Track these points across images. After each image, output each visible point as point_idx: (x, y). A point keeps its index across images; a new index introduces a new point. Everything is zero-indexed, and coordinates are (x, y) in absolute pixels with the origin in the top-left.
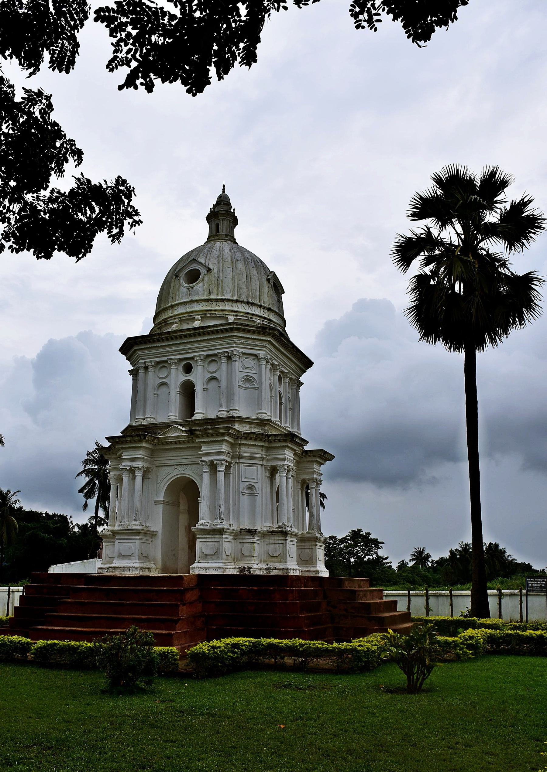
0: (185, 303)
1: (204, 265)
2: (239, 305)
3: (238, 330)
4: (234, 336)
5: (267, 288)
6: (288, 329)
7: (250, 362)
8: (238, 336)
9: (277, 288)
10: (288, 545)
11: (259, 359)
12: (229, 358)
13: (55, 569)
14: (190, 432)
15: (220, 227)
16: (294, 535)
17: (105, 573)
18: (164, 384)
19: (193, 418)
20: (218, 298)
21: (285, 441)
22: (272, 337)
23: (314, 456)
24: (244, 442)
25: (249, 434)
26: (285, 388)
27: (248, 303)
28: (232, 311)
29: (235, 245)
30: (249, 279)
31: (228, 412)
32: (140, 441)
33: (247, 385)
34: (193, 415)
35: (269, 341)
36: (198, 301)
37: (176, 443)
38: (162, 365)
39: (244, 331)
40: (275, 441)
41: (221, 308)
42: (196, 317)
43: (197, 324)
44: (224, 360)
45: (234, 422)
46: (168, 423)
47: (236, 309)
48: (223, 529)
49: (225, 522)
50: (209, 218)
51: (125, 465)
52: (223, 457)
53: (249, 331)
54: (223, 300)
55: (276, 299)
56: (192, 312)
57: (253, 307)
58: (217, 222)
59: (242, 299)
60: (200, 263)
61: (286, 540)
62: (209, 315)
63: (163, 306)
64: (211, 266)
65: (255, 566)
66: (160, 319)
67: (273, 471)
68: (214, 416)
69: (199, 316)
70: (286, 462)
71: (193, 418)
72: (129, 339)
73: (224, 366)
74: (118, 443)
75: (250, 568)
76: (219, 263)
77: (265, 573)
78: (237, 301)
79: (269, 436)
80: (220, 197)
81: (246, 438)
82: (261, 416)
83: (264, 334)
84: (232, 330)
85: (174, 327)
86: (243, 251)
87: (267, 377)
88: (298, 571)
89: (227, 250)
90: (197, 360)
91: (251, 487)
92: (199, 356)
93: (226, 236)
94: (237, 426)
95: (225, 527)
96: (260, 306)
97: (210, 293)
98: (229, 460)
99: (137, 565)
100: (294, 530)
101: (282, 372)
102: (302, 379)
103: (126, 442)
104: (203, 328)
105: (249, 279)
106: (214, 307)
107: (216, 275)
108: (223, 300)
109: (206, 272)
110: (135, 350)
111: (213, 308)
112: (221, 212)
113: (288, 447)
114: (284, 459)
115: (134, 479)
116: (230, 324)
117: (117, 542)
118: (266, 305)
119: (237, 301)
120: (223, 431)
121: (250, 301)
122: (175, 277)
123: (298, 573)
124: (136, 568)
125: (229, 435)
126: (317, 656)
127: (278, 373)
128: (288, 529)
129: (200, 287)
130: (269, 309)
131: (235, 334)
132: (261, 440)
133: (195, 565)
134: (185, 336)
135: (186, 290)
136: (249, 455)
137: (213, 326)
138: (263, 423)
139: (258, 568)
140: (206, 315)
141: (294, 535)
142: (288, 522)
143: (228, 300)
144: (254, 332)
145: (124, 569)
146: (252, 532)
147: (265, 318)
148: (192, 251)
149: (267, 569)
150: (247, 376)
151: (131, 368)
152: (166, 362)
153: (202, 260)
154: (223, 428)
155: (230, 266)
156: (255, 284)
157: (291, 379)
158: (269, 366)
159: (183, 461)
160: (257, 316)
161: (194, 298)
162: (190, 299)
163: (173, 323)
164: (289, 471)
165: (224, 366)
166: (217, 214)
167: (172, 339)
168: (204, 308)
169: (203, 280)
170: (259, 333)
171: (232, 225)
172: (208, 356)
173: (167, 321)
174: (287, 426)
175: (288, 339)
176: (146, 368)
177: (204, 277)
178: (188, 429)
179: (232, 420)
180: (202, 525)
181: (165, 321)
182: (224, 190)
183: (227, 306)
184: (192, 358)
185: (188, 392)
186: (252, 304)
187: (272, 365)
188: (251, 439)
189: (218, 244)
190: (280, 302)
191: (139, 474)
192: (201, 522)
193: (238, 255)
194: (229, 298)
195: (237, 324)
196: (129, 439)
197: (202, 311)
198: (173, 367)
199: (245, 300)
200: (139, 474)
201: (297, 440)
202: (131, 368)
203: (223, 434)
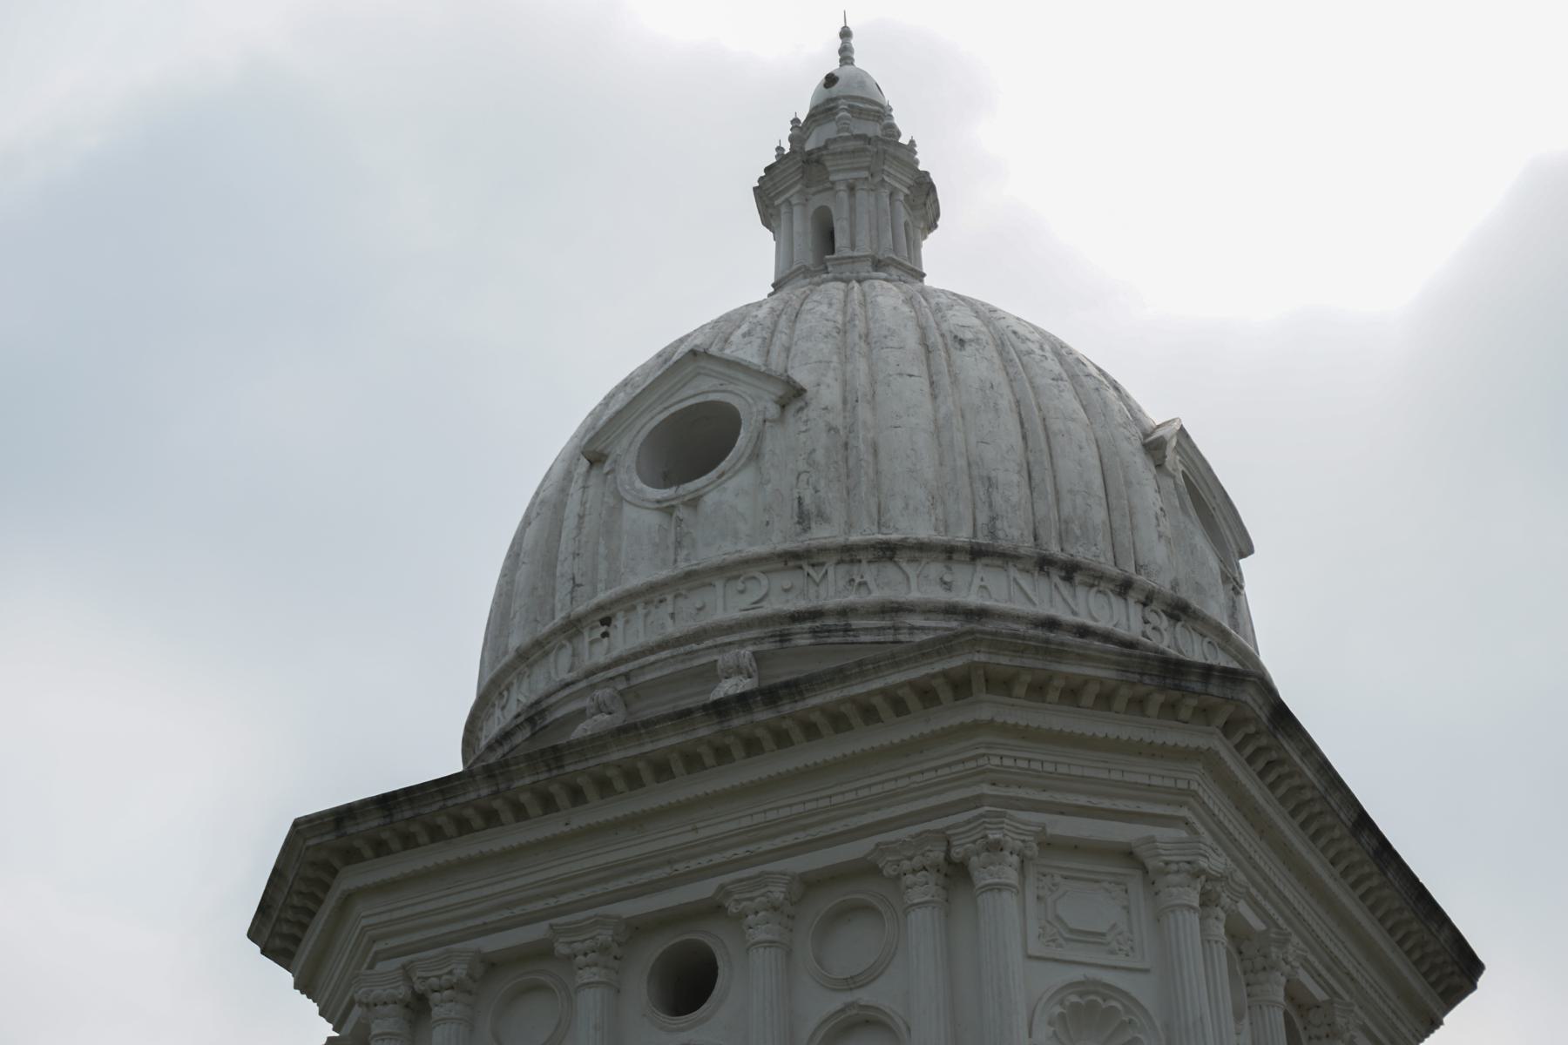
0: (651, 593)
3: (1001, 684)
4: (977, 726)
7: (1095, 906)
8: (1004, 729)
12: (956, 873)
20: (855, 538)
22: (1228, 729)
27: (1044, 564)
35: (1208, 759)
36: (731, 571)
39: (1038, 690)
41: (877, 595)
42: (725, 659)
47: (973, 599)
53: (1072, 694)
54: (887, 551)
56: (698, 636)
57: (1081, 592)
58: (818, 201)
59: (1003, 544)
62: (803, 641)
64: (802, 377)
69: (747, 651)
72: (302, 829)
73: (923, 925)
76: (846, 359)
78: (976, 553)
84: (961, 685)
90: (742, 915)
97: (804, 518)
107: (838, 422)
109: (773, 410)
110: (348, 898)
112: (837, 147)
119: (976, 553)
121: (1054, 549)
122: (585, 463)
131: (984, 713)
134: (662, 770)
135: (653, 519)
144: (1105, 700)
150: (1083, 987)
155: (919, 369)
161: (711, 554)
162: (683, 566)
165: (923, 925)
166: (818, 161)
167: (577, 796)
168: (779, 604)
169: (756, 455)
170: (1138, 704)
172: (812, 883)
173: (542, 713)
176: (418, 1007)
177: (760, 437)
182: (846, 55)
184: (714, 909)
190: (1234, 584)
194: (923, 531)
197: (763, 621)
198: (587, 975)
199: (1027, 546)
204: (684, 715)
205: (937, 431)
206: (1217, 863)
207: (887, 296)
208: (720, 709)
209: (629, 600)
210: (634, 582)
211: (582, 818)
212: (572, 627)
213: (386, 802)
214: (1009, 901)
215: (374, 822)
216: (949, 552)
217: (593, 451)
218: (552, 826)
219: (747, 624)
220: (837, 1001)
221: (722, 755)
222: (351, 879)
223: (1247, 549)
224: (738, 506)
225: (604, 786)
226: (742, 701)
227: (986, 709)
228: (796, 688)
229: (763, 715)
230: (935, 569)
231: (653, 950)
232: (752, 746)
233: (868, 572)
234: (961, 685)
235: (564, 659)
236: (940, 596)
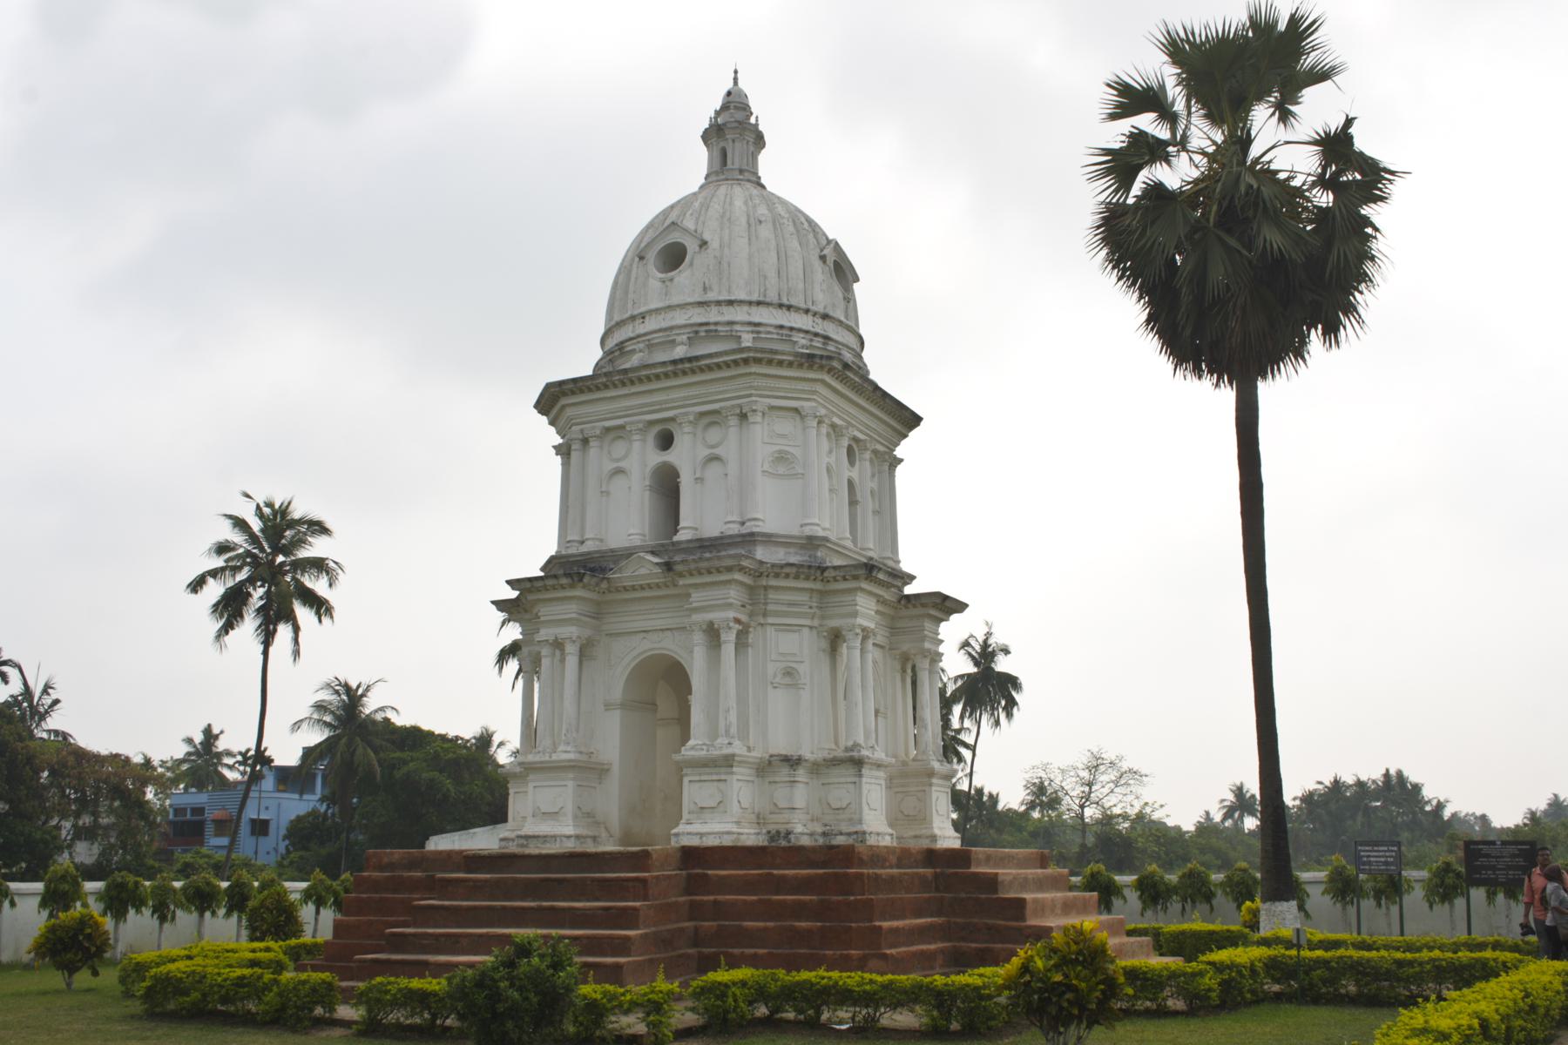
0: (657, 311)
1: (694, 234)
2: (762, 309)
3: (758, 361)
5: (820, 274)
6: (866, 355)
7: (785, 426)
9: (843, 272)
10: (865, 788)
11: (802, 417)
12: (743, 416)
13: (440, 843)
14: (668, 566)
15: (729, 155)
16: (879, 766)
17: (513, 848)
18: (619, 471)
19: (676, 538)
21: (855, 578)
23: (923, 605)
24: (773, 582)
25: (782, 566)
26: (862, 472)
27: (781, 306)
28: (750, 324)
29: (755, 191)
30: (782, 256)
31: (743, 524)
32: (572, 586)
33: (781, 470)
34: (676, 531)
35: (823, 382)
37: (642, 588)
38: (616, 433)
39: (770, 362)
40: (835, 579)
42: (679, 339)
43: (680, 352)
44: (733, 421)
45: (754, 543)
46: (627, 549)
47: (756, 319)
48: (733, 755)
49: (737, 743)
50: (706, 137)
51: (545, 634)
52: (731, 614)
53: (780, 363)
54: (730, 303)
55: (841, 295)
56: (672, 328)
58: (722, 144)
60: (686, 230)
61: (860, 776)
63: (617, 318)
64: (706, 237)
65: (799, 829)
66: (611, 343)
67: (835, 639)
68: (716, 533)
70: (860, 621)
71: (676, 538)
72: (549, 386)
73: (733, 432)
74: (530, 591)
75: (788, 833)
77: (821, 841)
78: (759, 303)
79: (824, 570)
80: (729, 93)
81: (777, 576)
82: (808, 531)
83: (811, 367)
84: (746, 361)
85: (634, 361)
86: (772, 201)
87: (820, 453)
88: (888, 838)
89: (739, 203)
91: (789, 673)
92: (686, 414)
93: (741, 171)
94: (761, 553)
95: (737, 751)
96: (807, 311)
97: (705, 289)
98: (744, 618)
99: (569, 831)
100: (880, 755)
101: (856, 439)
102: (899, 452)
103: (546, 589)
104: (690, 360)
105: (782, 256)
106: (713, 315)
108: (730, 303)
110: (563, 407)
111: (712, 320)
113: (862, 589)
114: (855, 614)
115: (563, 660)
116: (742, 350)
117: (531, 785)
118: (820, 308)
119: (759, 303)
120: (729, 562)
121: (785, 301)
123: (886, 841)
124: (569, 837)
125: (742, 569)
126: (895, 1006)
127: (845, 442)
128: (865, 753)
129: (682, 276)
130: (825, 317)
131: (753, 370)
132: (807, 578)
133: (681, 828)
134: (657, 377)
135: (659, 284)
136: (785, 608)
137: (710, 356)
138: (812, 543)
139: (804, 831)
140: (699, 332)
141: (879, 766)
142: (867, 737)
143: (741, 302)
144: (790, 364)
145: (545, 838)
146: (792, 762)
147: (816, 335)
148: (672, 207)
149: (824, 834)
150: (780, 452)
151: (558, 440)
152: (622, 427)
153: (689, 224)
154: (730, 556)
156: (796, 268)
157: (875, 452)
158: (824, 429)
159: (659, 624)
160: (800, 330)
161: (675, 300)
162: (667, 303)
163: (633, 351)
164: (865, 639)
165: (733, 432)
167: (632, 383)
169: (691, 264)
170: (801, 366)
171: (752, 148)
172: (703, 414)
174: (871, 549)
175: (862, 372)
176: (585, 441)
178: (666, 559)
179: (750, 539)
180: (692, 748)
181: (621, 346)
183: (739, 314)
184: (672, 419)
185: (667, 487)
186: (789, 307)
187: (833, 426)
188: (787, 576)
189: (723, 190)
190: (849, 299)
191: (571, 649)
192: (691, 743)
193: (762, 211)
194: (743, 296)
195: (756, 350)
196: (550, 582)
199: (776, 300)
200: (571, 649)
201: (881, 576)
202: (558, 440)
203: (729, 569)
204: (664, 364)
205: (750, 257)
206: (823, 412)
207: (739, 195)
208: (674, 362)
209: (650, 312)
210: (653, 306)
211: (634, 389)
212: (633, 318)
213: (574, 380)
214: (758, 428)
215: (571, 386)
216: (750, 303)
217: (638, 254)
218: (625, 391)
219: (685, 326)
220: (707, 452)
221: (675, 374)
222: (564, 401)
223: (857, 279)
224: (686, 282)
225: (640, 380)
226: (682, 360)
227: (754, 369)
228: (697, 358)
229: (687, 365)
230: (746, 308)
231: (657, 429)
232: (684, 373)
233: (725, 309)
234: (746, 361)
235: (631, 327)
236: (746, 318)
